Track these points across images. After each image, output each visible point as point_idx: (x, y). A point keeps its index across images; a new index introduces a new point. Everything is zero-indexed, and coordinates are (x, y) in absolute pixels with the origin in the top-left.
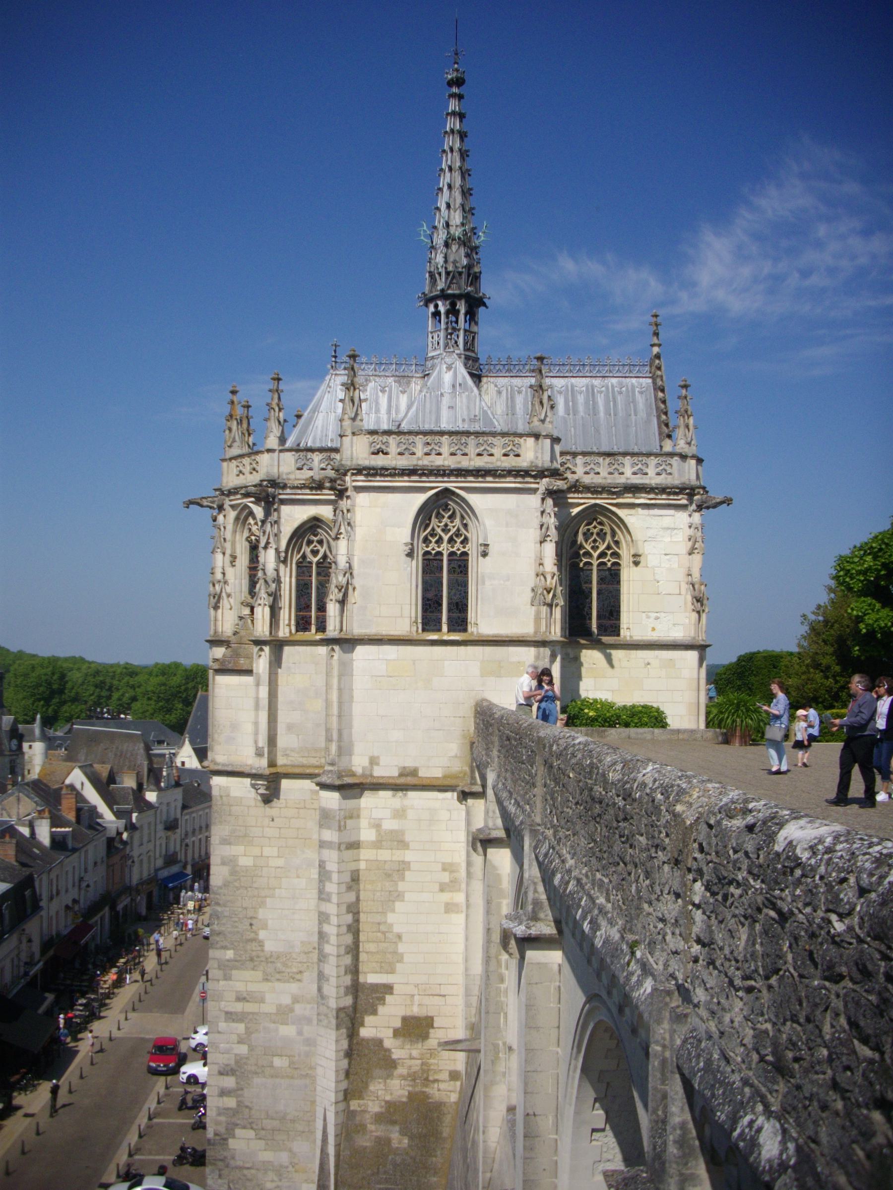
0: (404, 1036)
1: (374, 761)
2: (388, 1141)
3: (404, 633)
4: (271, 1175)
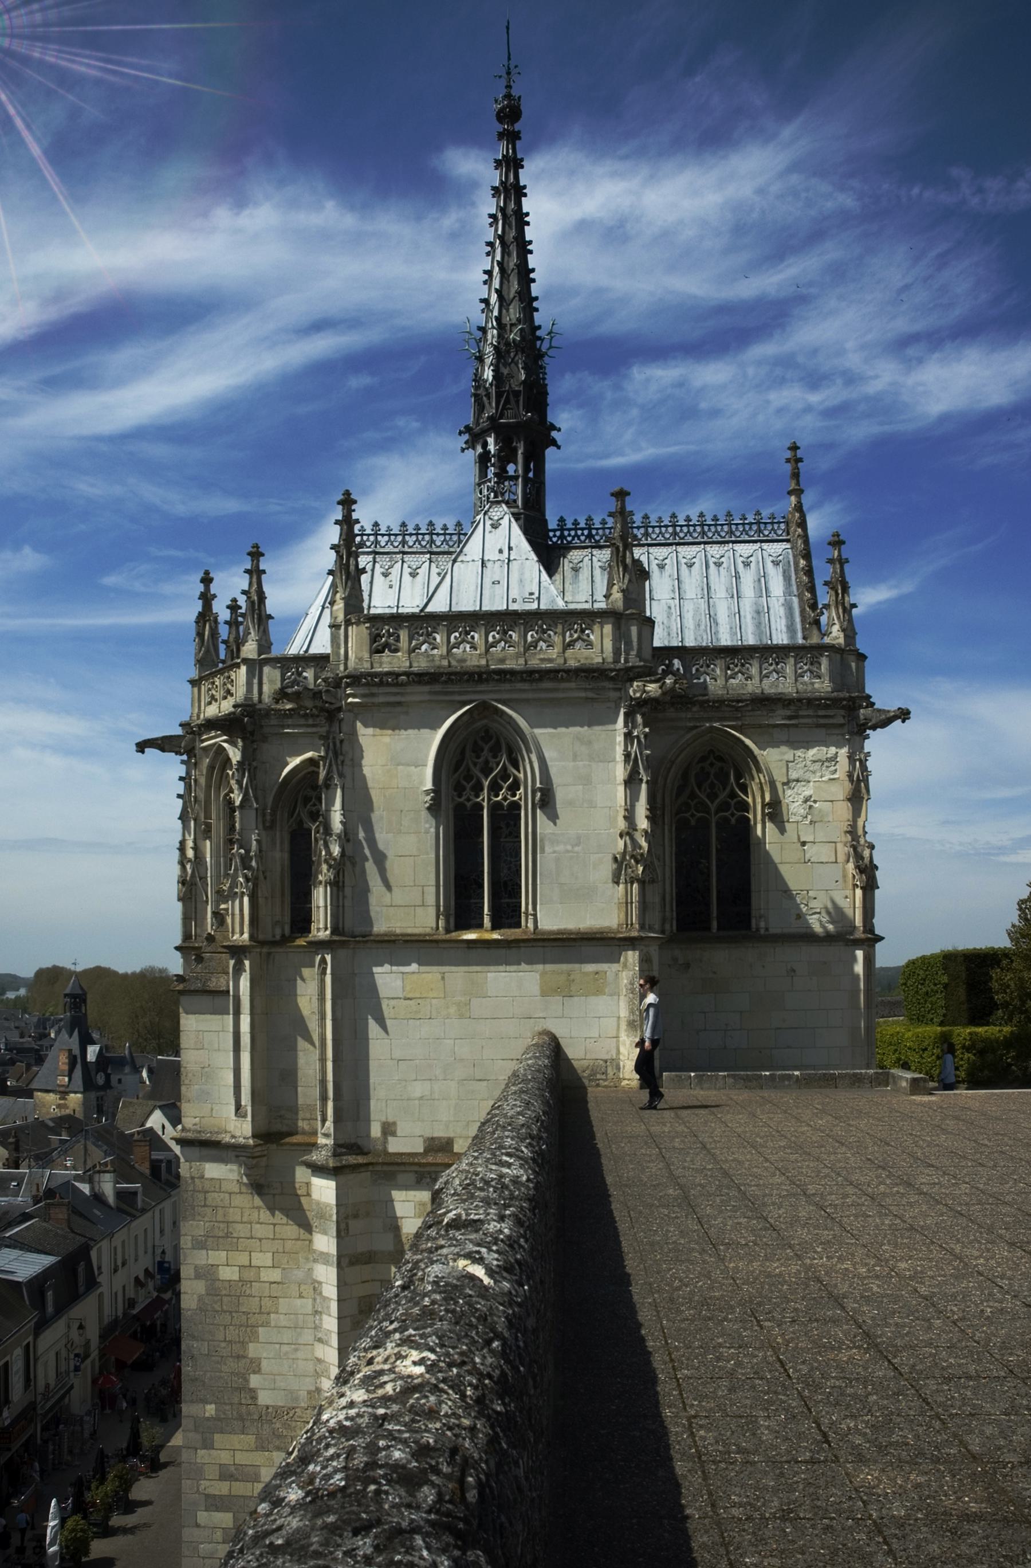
3: (428, 930)
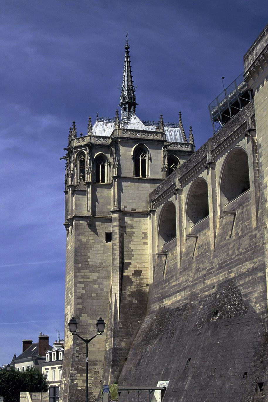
0: (135, 275)
1: (125, 207)
2: (132, 302)
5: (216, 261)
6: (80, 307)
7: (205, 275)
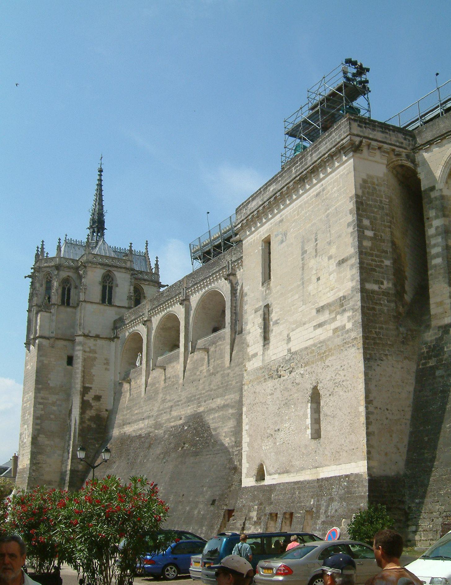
1: (90, 332)
4: (49, 448)
5: (184, 395)
6: (38, 427)
7: (172, 407)
